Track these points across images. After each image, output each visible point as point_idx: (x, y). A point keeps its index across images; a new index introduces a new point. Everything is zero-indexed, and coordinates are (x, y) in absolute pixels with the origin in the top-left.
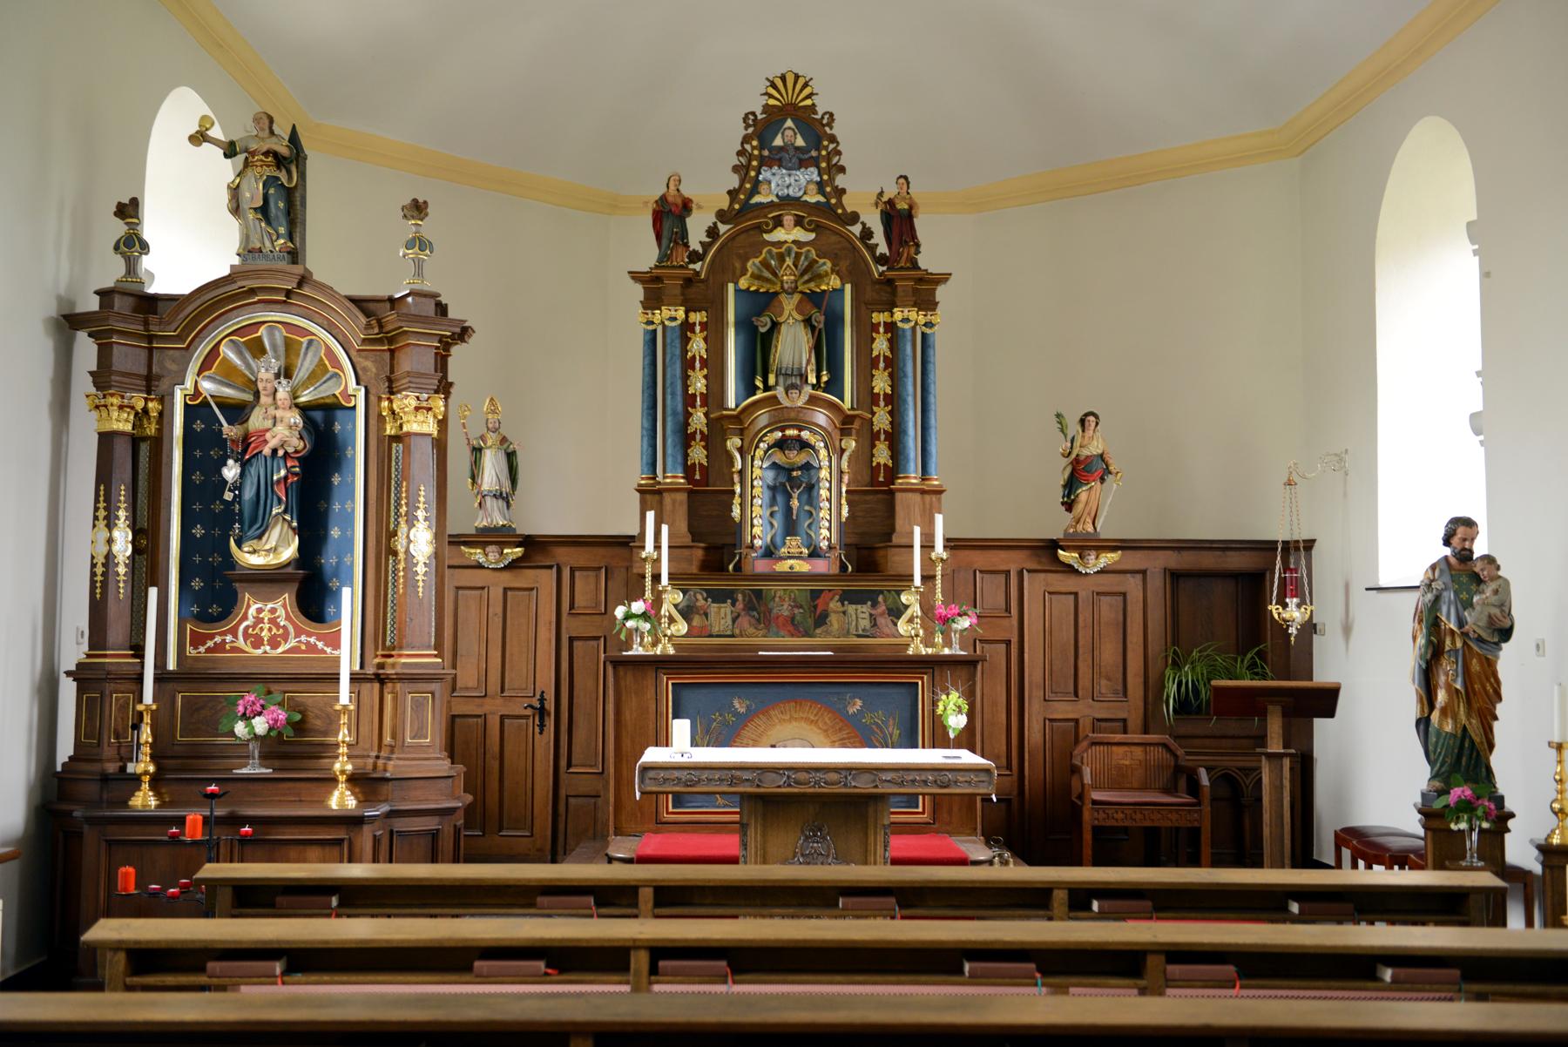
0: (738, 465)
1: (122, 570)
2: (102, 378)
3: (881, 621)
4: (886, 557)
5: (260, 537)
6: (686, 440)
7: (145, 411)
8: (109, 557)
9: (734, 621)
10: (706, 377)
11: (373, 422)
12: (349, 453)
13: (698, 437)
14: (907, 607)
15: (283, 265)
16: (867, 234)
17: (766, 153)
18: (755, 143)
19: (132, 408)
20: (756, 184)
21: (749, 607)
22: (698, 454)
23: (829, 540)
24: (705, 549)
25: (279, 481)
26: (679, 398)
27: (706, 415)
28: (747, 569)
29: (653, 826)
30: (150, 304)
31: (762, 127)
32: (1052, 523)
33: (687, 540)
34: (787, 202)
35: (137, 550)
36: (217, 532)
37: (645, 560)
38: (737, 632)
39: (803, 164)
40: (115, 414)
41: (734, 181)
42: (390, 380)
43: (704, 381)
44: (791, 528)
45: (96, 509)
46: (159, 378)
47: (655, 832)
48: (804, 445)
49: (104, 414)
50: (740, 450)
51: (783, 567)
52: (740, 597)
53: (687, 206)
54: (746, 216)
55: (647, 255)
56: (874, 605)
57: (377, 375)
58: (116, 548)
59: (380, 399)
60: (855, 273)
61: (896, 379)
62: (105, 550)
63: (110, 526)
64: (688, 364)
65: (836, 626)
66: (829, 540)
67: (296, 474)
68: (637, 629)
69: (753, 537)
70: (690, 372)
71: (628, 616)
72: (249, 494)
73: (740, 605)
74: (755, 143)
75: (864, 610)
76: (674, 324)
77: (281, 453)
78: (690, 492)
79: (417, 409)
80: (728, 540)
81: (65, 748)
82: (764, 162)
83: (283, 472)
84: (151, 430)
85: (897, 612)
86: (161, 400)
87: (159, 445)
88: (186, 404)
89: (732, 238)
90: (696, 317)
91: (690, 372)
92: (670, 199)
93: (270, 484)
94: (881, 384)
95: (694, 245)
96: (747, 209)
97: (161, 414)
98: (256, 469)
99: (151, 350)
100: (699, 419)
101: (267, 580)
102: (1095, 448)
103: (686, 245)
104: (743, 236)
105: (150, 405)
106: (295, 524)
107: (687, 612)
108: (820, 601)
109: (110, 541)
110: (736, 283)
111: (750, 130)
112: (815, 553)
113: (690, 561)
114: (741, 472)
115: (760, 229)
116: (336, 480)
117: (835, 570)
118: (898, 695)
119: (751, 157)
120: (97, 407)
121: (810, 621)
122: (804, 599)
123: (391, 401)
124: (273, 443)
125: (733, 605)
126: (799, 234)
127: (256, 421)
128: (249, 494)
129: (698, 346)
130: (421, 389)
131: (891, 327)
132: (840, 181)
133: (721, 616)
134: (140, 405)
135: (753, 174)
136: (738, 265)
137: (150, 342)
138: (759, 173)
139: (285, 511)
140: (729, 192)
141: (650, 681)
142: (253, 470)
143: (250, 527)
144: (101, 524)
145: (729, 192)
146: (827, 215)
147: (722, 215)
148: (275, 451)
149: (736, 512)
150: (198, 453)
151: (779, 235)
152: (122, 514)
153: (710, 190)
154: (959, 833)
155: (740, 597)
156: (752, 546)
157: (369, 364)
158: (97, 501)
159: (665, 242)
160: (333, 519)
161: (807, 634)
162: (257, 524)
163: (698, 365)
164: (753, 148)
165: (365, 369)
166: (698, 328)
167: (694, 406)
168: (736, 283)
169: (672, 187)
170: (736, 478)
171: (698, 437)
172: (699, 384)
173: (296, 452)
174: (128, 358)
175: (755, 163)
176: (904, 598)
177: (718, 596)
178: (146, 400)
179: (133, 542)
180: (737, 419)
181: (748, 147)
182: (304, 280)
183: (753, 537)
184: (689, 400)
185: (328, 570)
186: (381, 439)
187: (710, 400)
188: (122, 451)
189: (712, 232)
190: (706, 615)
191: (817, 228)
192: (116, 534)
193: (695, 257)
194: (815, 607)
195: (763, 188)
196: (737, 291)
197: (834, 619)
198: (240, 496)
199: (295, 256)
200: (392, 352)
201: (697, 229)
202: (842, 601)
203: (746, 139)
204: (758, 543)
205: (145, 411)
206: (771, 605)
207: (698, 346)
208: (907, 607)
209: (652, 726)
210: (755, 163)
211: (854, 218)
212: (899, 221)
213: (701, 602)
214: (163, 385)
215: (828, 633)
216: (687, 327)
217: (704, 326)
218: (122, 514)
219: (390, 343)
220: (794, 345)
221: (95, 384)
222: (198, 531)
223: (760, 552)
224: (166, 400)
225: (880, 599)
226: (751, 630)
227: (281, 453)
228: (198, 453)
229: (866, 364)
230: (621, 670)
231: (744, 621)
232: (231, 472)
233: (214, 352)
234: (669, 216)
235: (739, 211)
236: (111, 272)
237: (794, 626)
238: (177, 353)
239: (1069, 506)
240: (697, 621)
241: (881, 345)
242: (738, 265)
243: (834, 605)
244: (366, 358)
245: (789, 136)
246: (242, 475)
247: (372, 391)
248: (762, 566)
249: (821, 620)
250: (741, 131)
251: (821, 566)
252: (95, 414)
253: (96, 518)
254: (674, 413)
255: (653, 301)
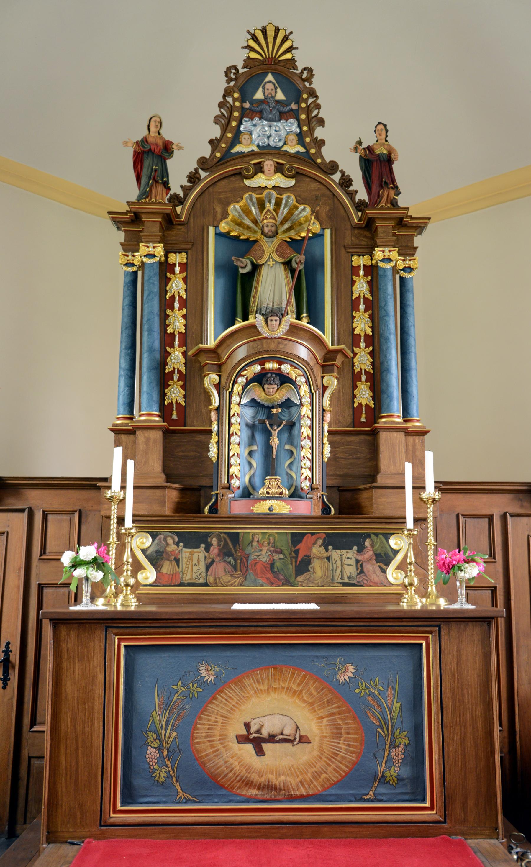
0: (216, 402)
3: (369, 568)
4: (371, 498)
6: (163, 379)
9: (208, 567)
10: (184, 317)
13: (176, 376)
14: (396, 552)
16: (346, 182)
17: (247, 105)
18: (236, 95)
20: (237, 134)
21: (225, 552)
22: (175, 393)
23: (311, 480)
24: (181, 490)
26: (156, 335)
27: (184, 354)
28: (223, 511)
29: (96, 829)
31: (242, 83)
33: (161, 480)
34: (267, 151)
37: (111, 499)
38: (211, 579)
39: (283, 116)
41: (216, 132)
43: (183, 321)
44: (270, 467)
47: (98, 837)
48: (285, 380)
50: (218, 386)
51: (262, 508)
52: (215, 541)
53: (167, 149)
54: (226, 165)
55: (126, 190)
56: (361, 549)
60: (334, 217)
61: (376, 320)
64: (166, 304)
65: (319, 573)
66: (311, 480)
68: (87, 579)
69: (230, 477)
70: (169, 312)
71: (76, 564)
73: (214, 550)
74: (236, 95)
75: (351, 554)
76: (152, 261)
78: (167, 433)
80: (204, 482)
82: (244, 114)
85: (384, 558)
89: (213, 184)
90: (176, 258)
91: (169, 312)
92: (150, 140)
94: (362, 325)
95: (176, 189)
96: (227, 157)
100: (177, 359)
103: (166, 186)
104: (223, 183)
107: (156, 559)
108: (301, 546)
110: (216, 227)
111: (232, 84)
112: (296, 494)
113: (163, 503)
114: (218, 409)
115: (239, 175)
117: (317, 511)
118: (398, 660)
119: (231, 109)
121: (291, 568)
122: (284, 543)
125: (207, 549)
126: (279, 180)
129: (177, 286)
131: (372, 271)
132: (319, 133)
133: (193, 562)
135: (234, 124)
136: (219, 209)
138: (240, 123)
140: (211, 142)
141: (98, 644)
145: (211, 142)
146: (307, 166)
147: (203, 163)
149: (213, 451)
151: (260, 180)
153: (192, 142)
154: (476, 835)
155: (215, 541)
156: (229, 487)
159: (144, 180)
161: (287, 582)
163: (177, 305)
164: (235, 100)
166: (177, 269)
167: (172, 346)
168: (216, 227)
169: (152, 128)
170: (213, 416)
171: (176, 376)
172: (177, 323)
175: (236, 114)
176: (393, 542)
177: (190, 540)
180: (214, 352)
181: (230, 100)
183: (230, 477)
184: (167, 340)
187: (189, 340)
189: (193, 178)
190: (177, 561)
191: (297, 175)
193: (176, 200)
194: (297, 552)
195: (244, 138)
196: (219, 235)
197: (317, 565)
201: (179, 171)
202: (325, 545)
203: (227, 93)
204: (235, 483)
206: (248, 550)
208: (396, 552)
209: (98, 700)
210: (236, 114)
211: (333, 167)
212: (378, 166)
213: (172, 547)
215: (311, 581)
216: (165, 269)
217: (184, 267)
220: (273, 285)
223: (238, 493)
225: (367, 543)
226: (227, 578)
229: (347, 306)
230: (63, 632)
231: (219, 568)
234: (151, 157)
235: (221, 159)
237: (273, 573)
240: (167, 568)
241: (361, 288)
242: (219, 209)
243: (317, 550)
245: (269, 89)
248: (239, 508)
249: (303, 566)
250: (222, 84)
251: (303, 508)
254: (151, 350)
255: (131, 246)
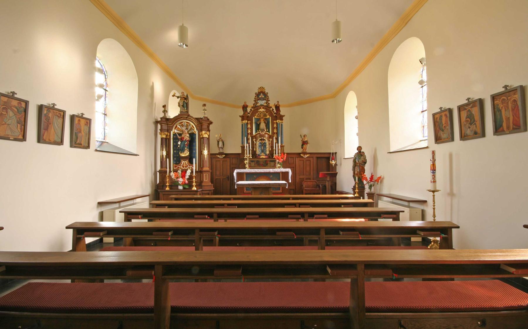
2: (161, 130)
8: (163, 155)
15: (186, 113)
16: (273, 110)
21: (257, 163)
30: (168, 120)
31: (258, 95)
32: (300, 151)
34: (261, 105)
35: (167, 154)
39: (264, 100)
41: (254, 102)
44: (262, 151)
48: (264, 140)
54: (256, 108)
55: (242, 113)
60: (271, 115)
61: (277, 130)
64: (248, 129)
72: (182, 146)
81: (158, 182)
82: (258, 100)
87: (169, 139)
89: (254, 110)
90: (249, 122)
94: (275, 131)
95: (248, 112)
96: (256, 106)
98: (183, 143)
101: (185, 158)
102: (306, 140)
115: (258, 109)
126: (263, 110)
127: (183, 136)
129: (249, 126)
131: (277, 123)
132: (269, 102)
146: (267, 107)
147: (252, 107)
151: (260, 110)
153: (251, 104)
162: (183, 150)
172: (249, 131)
174: (165, 127)
180: (255, 136)
182: (189, 115)
188: (164, 141)
189: (251, 110)
191: (266, 109)
193: (249, 113)
199: (187, 112)
201: (249, 110)
207: (249, 126)
211: (271, 107)
212: (277, 108)
216: (247, 123)
220: (263, 125)
224: (170, 133)
229: (273, 128)
232: (179, 143)
233: (176, 126)
234: (245, 107)
236: (162, 115)
239: (302, 148)
241: (275, 126)
245: (262, 96)
250: (255, 95)
255: (242, 120)
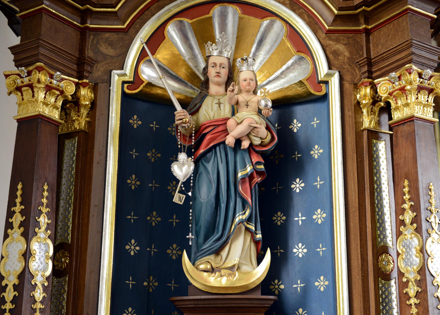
1: (39, 294)
5: (217, 252)
7: (76, 97)
8: (25, 276)
11: (349, 113)
12: (317, 152)
19: (62, 92)
25: (243, 179)
36: (154, 250)
40: (41, 95)
42: (370, 63)
45: (10, 214)
46: (93, 63)
49: (27, 92)
57: (351, 60)
58: (34, 265)
59: (356, 87)
62: (19, 267)
63: (27, 236)
67: (259, 173)
72: (205, 194)
77: (245, 144)
79: (420, 89)
83: (249, 169)
84: (81, 122)
86: (94, 89)
87: (89, 142)
88: (123, 93)
93: (233, 182)
97: (93, 104)
98: (215, 165)
99: (84, 32)
105: (84, 92)
106: (259, 236)
109: (27, 255)
116: (297, 186)
120: (19, 89)
123: (374, 88)
124: (235, 131)
127: (209, 111)
128: (205, 194)
130: (423, 65)
134: (70, 90)
137: (83, 22)
139: (249, 220)
142: (210, 166)
143: (206, 238)
144: (16, 233)
148: (238, 142)
150: (134, 154)
152: (43, 220)
157: (340, 47)
158: (11, 203)
160: (294, 234)
165: (336, 53)
173: (262, 145)
178: (77, 85)
179: (54, 258)
185: (290, 299)
186: (358, 134)
188: (47, 144)
192: (35, 246)
198: (194, 198)
200: (368, 32)
205: (76, 97)
214: (98, 72)
218: (43, 220)
219: (367, 22)
221: (18, 63)
222: (133, 248)
224: (100, 87)
227: (245, 144)
228: (134, 154)
232: (182, 168)
238: (114, 37)
244: (337, 41)
246: (196, 171)
247: (348, 77)
252: (15, 98)
253: (9, 225)
